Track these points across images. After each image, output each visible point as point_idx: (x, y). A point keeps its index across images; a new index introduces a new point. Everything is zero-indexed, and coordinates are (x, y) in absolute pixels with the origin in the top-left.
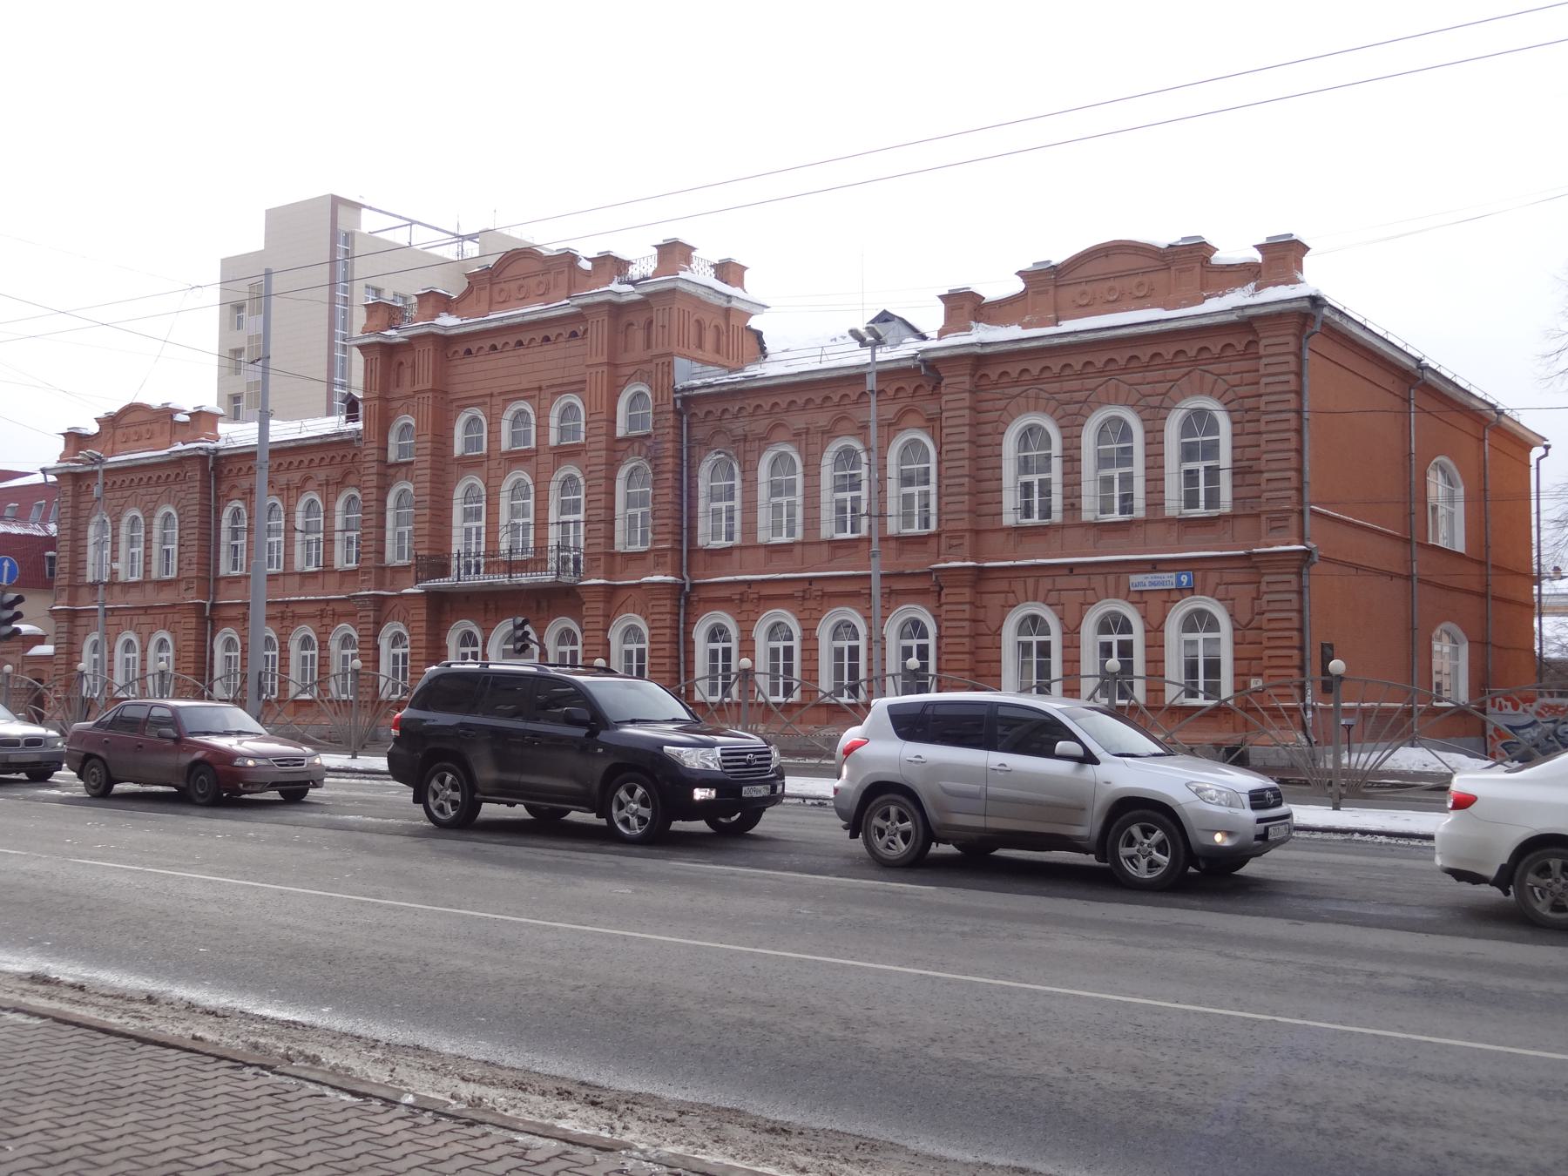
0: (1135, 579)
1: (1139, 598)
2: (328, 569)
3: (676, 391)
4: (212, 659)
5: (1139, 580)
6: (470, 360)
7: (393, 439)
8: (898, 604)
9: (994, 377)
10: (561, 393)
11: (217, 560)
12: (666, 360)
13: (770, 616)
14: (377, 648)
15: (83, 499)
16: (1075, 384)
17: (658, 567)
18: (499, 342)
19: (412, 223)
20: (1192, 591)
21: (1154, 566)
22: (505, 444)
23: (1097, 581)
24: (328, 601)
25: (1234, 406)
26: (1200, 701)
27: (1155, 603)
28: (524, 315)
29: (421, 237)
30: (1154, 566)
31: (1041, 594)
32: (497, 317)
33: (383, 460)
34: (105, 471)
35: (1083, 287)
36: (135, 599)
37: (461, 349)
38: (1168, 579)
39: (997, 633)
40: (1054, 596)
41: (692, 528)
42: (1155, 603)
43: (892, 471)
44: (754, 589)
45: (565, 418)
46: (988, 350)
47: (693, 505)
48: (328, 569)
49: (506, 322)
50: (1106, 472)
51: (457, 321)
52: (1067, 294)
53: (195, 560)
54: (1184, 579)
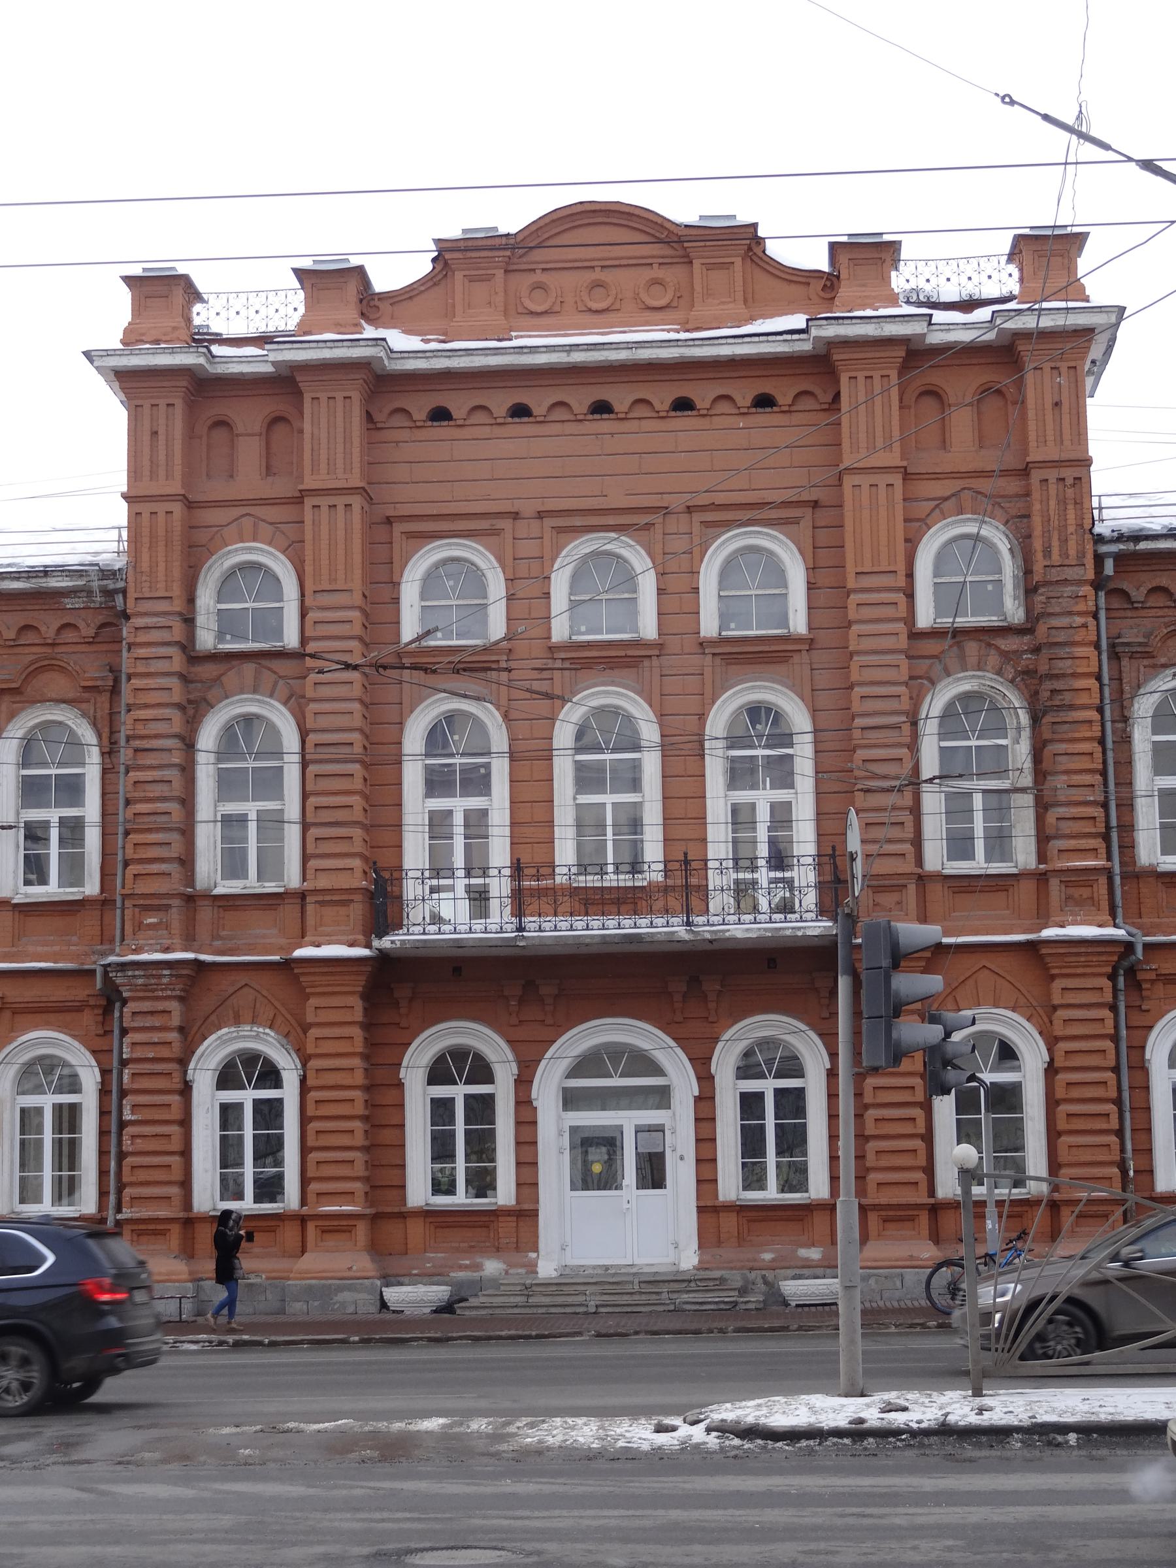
3: (1100, 539)
6: (441, 430)
7: (206, 598)
10: (728, 525)
12: (1069, 473)
14: (186, 1090)
17: (1079, 907)
22: (709, 626)
28: (629, 346)
32: (538, 344)
33: (187, 646)
41: (1128, 828)
45: (759, 579)
47: (1126, 781)
49: (578, 357)
51: (413, 343)
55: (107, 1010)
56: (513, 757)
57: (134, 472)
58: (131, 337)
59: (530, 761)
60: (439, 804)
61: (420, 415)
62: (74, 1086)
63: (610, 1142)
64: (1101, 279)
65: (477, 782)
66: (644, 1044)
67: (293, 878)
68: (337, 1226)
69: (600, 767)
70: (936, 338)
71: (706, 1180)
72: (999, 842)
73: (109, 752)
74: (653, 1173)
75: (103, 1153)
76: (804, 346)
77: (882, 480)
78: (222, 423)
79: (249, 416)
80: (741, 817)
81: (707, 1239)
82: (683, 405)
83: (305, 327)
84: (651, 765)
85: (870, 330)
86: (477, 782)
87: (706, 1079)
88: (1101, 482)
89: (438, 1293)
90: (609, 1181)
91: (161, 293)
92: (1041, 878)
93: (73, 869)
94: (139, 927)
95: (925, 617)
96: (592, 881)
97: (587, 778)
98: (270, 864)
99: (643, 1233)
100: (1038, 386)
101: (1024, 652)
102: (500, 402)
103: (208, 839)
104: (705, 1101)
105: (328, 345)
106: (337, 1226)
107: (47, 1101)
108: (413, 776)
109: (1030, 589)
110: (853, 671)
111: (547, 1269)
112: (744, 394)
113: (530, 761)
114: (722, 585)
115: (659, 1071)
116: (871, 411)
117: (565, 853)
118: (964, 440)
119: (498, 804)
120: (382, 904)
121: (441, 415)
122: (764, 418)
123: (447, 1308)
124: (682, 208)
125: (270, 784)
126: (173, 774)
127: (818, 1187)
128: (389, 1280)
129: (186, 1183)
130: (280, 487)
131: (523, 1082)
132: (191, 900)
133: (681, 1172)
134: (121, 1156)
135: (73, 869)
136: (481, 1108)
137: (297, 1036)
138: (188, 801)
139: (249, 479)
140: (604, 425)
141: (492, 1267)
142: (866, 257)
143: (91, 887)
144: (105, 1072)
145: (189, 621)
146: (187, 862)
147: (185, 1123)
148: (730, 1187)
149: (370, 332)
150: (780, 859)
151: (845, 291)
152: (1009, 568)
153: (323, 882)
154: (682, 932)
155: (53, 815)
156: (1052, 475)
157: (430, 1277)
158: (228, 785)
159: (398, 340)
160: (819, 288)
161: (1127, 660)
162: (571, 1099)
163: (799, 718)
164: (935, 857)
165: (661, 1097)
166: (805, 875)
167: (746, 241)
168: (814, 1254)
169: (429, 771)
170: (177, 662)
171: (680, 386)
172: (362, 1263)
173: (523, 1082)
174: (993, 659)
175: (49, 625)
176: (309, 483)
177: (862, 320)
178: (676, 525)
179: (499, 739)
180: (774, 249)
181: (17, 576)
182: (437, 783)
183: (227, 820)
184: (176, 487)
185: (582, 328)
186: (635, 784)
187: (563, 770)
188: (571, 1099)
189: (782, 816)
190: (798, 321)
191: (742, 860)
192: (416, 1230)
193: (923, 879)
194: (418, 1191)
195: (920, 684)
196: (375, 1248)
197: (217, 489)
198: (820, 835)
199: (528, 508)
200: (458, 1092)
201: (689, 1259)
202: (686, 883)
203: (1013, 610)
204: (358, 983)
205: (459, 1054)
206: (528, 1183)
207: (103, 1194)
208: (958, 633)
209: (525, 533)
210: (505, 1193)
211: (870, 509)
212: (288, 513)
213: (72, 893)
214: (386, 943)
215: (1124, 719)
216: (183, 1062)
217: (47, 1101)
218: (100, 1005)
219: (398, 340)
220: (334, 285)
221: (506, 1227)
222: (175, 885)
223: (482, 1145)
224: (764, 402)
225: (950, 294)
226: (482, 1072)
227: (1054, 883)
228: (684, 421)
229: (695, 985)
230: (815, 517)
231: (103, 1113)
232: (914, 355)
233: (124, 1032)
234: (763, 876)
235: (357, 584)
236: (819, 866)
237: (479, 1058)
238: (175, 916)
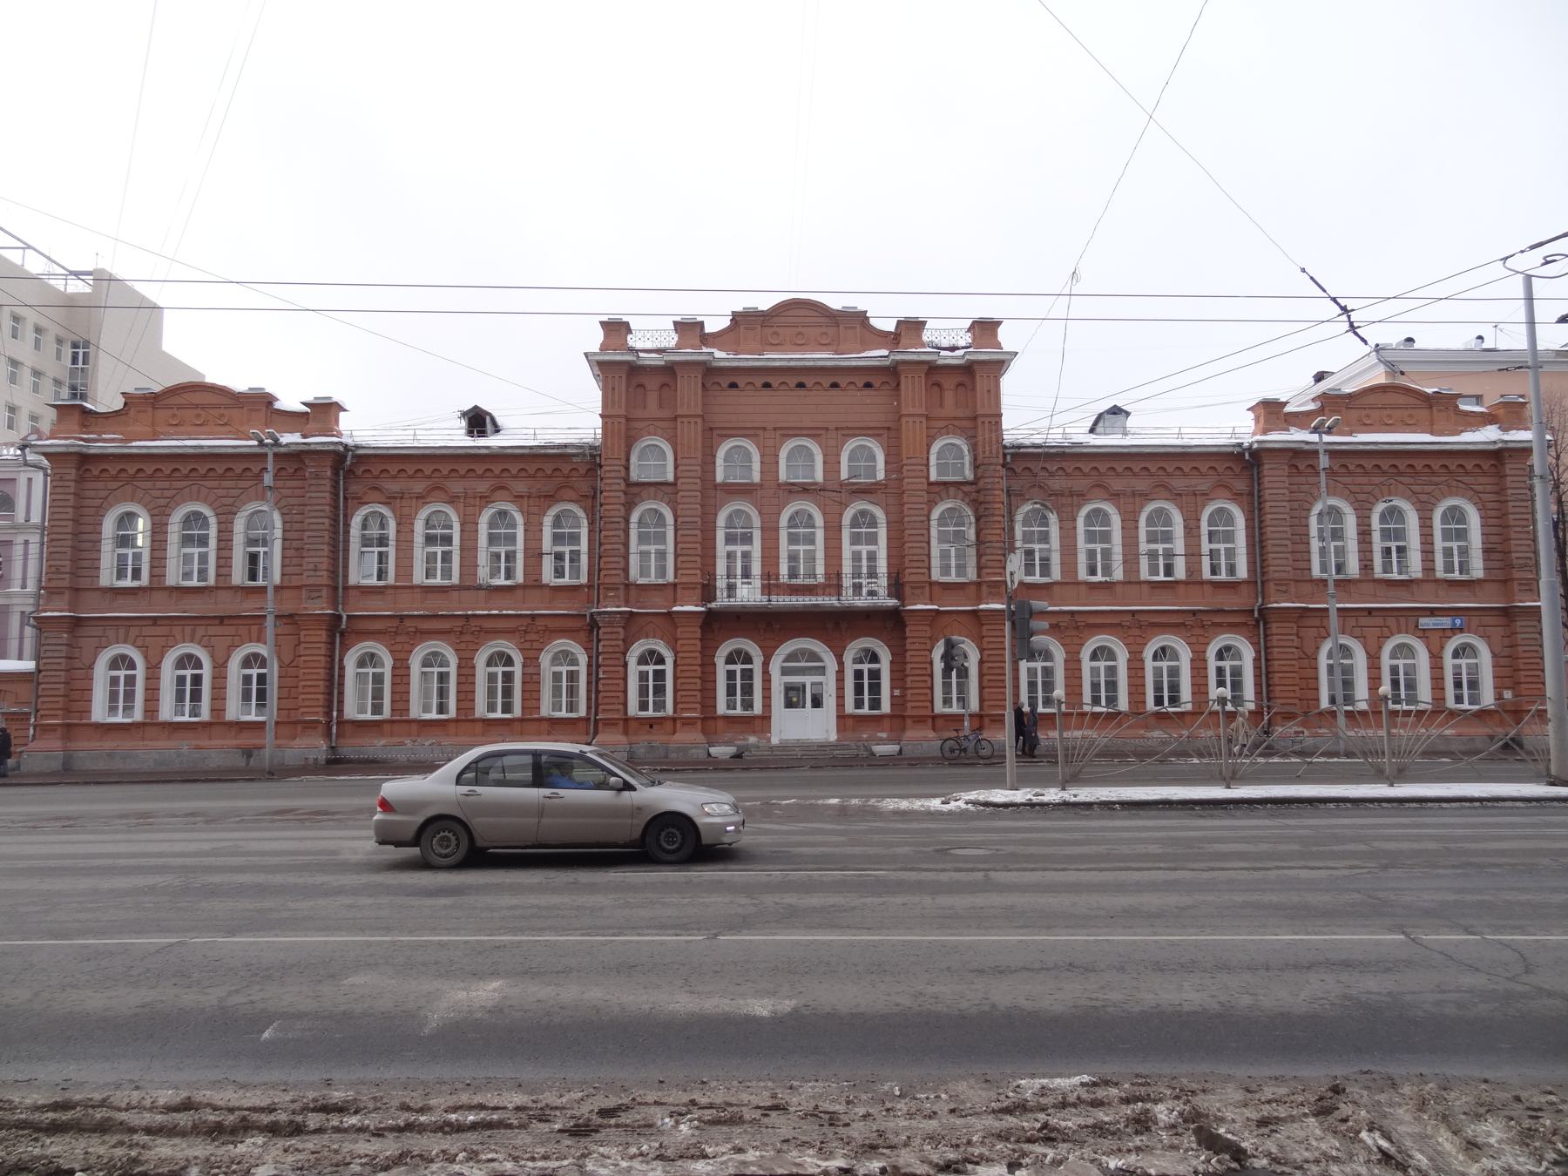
0: (1422, 621)
1: (1424, 634)
2: (533, 584)
3: (1005, 447)
4: (342, 676)
5: (1426, 622)
6: (734, 392)
7: (634, 459)
8: (1218, 634)
11: (346, 567)
12: (993, 420)
14: (625, 665)
15: (89, 485)
16: (1364, 480)
19: (29, 247)
20: (1461, 630)
21: (1432, 612)
23: (1391, 622)
24: (533, 617)
26: (1466, 706)
29: (35, 265)
30: (1432, 612)
33: (626, 479)
34: (276, 455)
35: (1388, 412)
36: (197, 607)
37: (725, 382)
38: (1446, 622)
40: (1358, 631)
43: (1205, 528)
44: (1077, 618)
45: (868, 458)
46: (1307, 447)
48: (533, 584)
49: (792, 364)
50: (495, 549)
52: (1354, 414)
53: (325, 566)
54: (1458, 622)
55: (591, 631)
56: (763, 529)
57: (605, 406)
58: (604, 347)
59: (770, 532)
60: (730, 548)
61: (725, 385)
62: (574, 662)
63: (801, 689)
64: (1007, 338)
65: (747, 539)
66: (816, 649)
67: (670, 577)
68: (689, 722)
69: (797, 534)
70: (940, 362)
71: (840, 704)
72: (961, 569)
73: (591, 523)
74: (817, 702)
75: (589, 691)
76: (887, 363)
77: (918, 420)
78: (641, 386)
79: (652, 383)
80: (856, 557)
81: (841, 728)
82: (835, 385)
83: (679, 346)
84: (820, 535)
85: (915, 357)
86: (747, 539)
87: (841, 663)
88: (1006, 423)
89: (732, 750)
91: (616, 329)
92: (978, 584)
93: (576, 572)
94: (606, 597)
95: (933, 477)
96: (794, 581)
97: (793, 539)
98: (662, 571)
99: (813, 726)
100: (981, 384)
101: (974, 492)
102: (759, 381)
103: (634, 560)
104: (840, 673)
105: (689, 354)
106: (689, 722)
107: (564, 669)
108: (720, 536)
109: (976, 466)
110: (903, 497)
111: (775, 741)
112: (860, 382)
113: (770, 532)
114: (850, 460)
115: (820, 660)
116: (913, 391)
117: (784, 570)
118: (950, 404)
119: (756, 549)
120: (708, 592)
121: (733, 385)
122: (867, 392)
123: (738, 756)
124: (835, 303)
125: (661, 538)
126: (621, 533)
127: (886, 707)
128: (711, 744)
129: (625, 704)
130: (666, 413)
131: (766, 664)
132: (627, 586)
133: (830, 701)
134: (598, 692)
135: (576, 572)
136: (748, 675)
137: (673, 644)
138: (626, 544)
139: (653, 409)
140: (802, 392)
141: (752, 739)
142: (911, 327)
143: (584, 580)
145: (627, 468)
146: (626, 570)
147: (625, 679)
148: (850, 707)
149: (705, 350)
150: (872, 574)
151: (903, 341)
152: (967, 459)
153: (684, 580)
154: (836, 603)
155: (566, 549)
156: (987, 420)
157: (727, 743)
158: (643, 538)
159: (719, 354)
160: (892, 339)
161: (1014, 497)
162: (785, 672)
163: (880, 514)
164: (936, 575)
165: (821, 671)
166: (883, 581)
167: (861, 318)
168: (884, 735)
169: (727, 535)
170: (623, 486)
171: (834, 378)
172: (700, 738)
173: (766, 664)
174: (961, 495)
175: (566, 468)
176: (680, 412)
177: (912, 353)
178: (831, 435)
179: (757, 522)
180: (872, 321)
181: (553, 447)
182: (730, 539)
183: (641, 553)
184: (622, 412)
185: (794, 351)
186: (812, 542)
187: (783, 536)
188: (785, 672)
189: (872, 557)
190: (885, 352)
191: (857, 574)
192: (720, 724)
193: (932, 584)
194: (721, 708)
195: (932, 504)
196: (704, 731)
197: (639, 414)
198: (889, 565)
199: (769, 426)
200: (738, 668)
201: (833, 737)
202: (834, 583)
203: (969, 475)
204: (699, 622)
205: (739, 652)
206: (767, 705)
207: (589, 708)
208: (945, 484)
209: (769, 436)
210: (758, 709)
211: (912, 431)
212: (671, 426)
213: (575, 582)
214: (713, 605)
215: (1012, 521)
216: (625, 654)
217: (564, 669)
218: (589, 629)
219: (719, 354)
220: (689, 329)
221: (757, 722)
222: (621, 580)
223: (748, 690)
224: (868, 385)
225: (945, 344)
226: (748, 659)
227: (984, 588)
228: (834, 392)
229: (836, 625)
230: (890, 434)
231: (589, 674)
232: (933, 370)
233: (599, 641)
235: (699, 454)
236: (889, 577)
237: (747, 654)
238: (622, 593)
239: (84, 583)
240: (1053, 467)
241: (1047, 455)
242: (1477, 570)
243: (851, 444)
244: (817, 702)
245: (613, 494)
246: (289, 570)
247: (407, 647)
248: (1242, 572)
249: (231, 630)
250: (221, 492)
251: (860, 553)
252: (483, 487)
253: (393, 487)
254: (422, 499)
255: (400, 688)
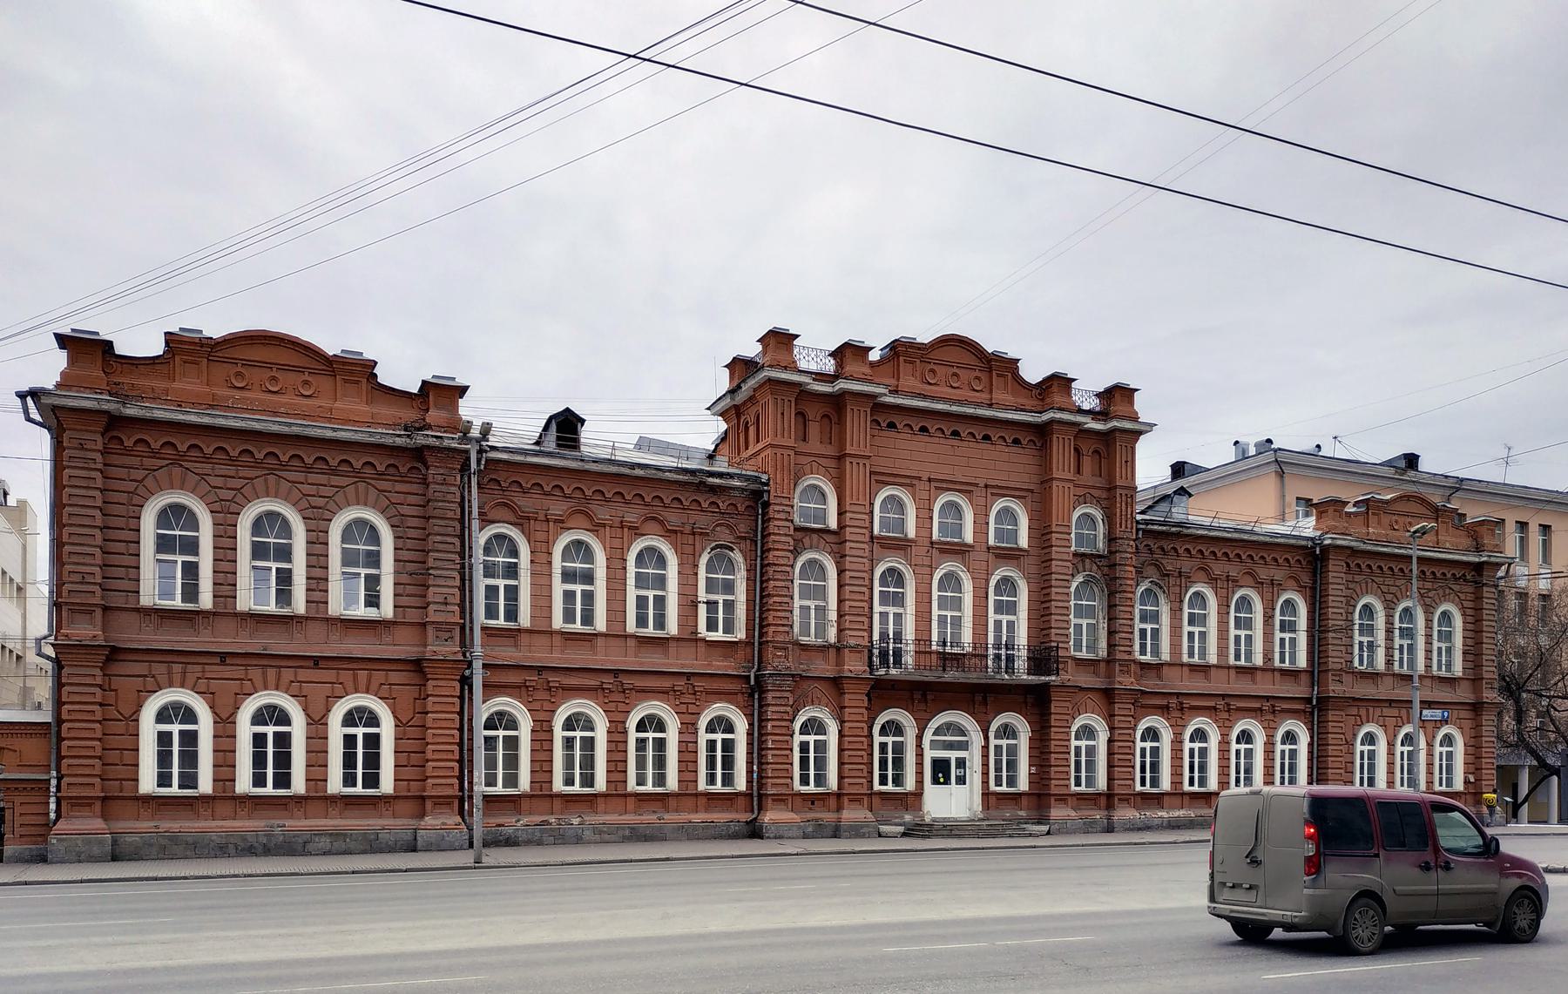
2: (689, 638)
9: (129, 443)
13: (579, 705)
18: (933, 426)
25: (217, 506)
27: (1430, 726)
31: (374, 686)
39: (134, 719)
42: (1430, 726)
48: (689, 638)
71: (985, 782)
75: (750, 763)
77: (1067, 485)
87: (986, 738)
90: (947, 782)
131: (919, 738)
143: (740, 634)
144: (751, 725)
148: (993, 787)
152: (1101, 529)
162: (934, 745)
173: (919, 738)
207: (749, 782)
208: (1083, 555)
234: (1003, 652)
239: (117, 600)
240: (1168, 546)
241: (1178, 535)
242: (1458, 669)
243: (999, 504)
244: (961, 780)
245: (780, 537)
246: (405, 601)
247: (547, 706)
248: (1302, 662)
249: (329, 675)
250: (306, 488)
251: (573, 593)
252: (632, 517)
253: (526, 503)
254: (562, 524)
255: (542, 756)
